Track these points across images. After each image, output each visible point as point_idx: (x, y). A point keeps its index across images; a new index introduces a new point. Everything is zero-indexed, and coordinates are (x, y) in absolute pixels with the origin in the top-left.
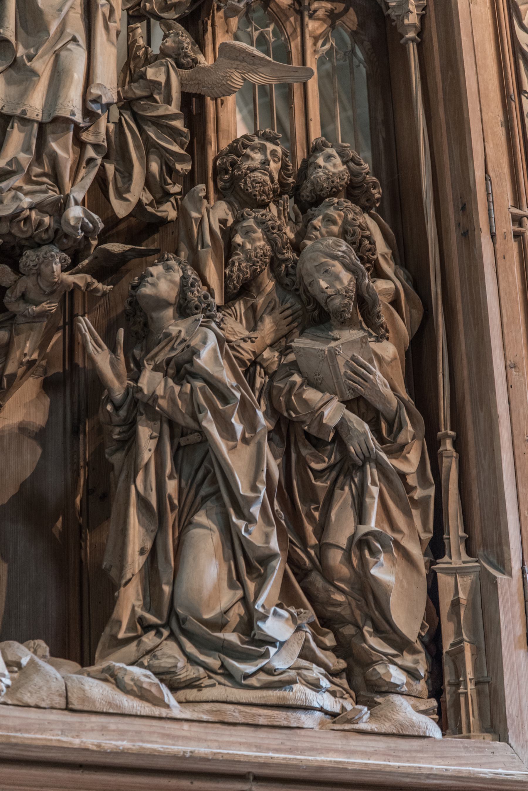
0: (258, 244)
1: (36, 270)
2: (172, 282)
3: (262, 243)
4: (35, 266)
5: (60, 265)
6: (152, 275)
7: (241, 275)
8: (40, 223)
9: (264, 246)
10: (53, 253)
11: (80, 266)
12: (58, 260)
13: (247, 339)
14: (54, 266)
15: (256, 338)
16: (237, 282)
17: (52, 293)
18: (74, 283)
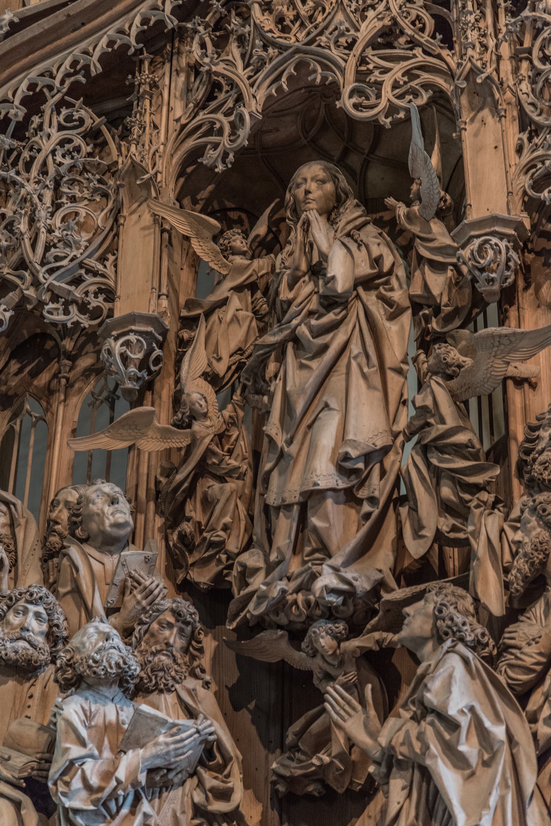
0: (534, 533)
1: (312, 649)
2: (426, 615)
3: (539, 530)
4: (308, 647)
5: (329, 637)
6: (408, 615)
7: (519, 575)
8: (308, 603)
9: (539, 534)
10: (314, 629)
11: (368, 626)
12: (324, 634)
13: (532, 642)
14: (321, 640)
15: (540, 637)
16: (518, 584)
17: (342, 663)
18: (358, 647)
